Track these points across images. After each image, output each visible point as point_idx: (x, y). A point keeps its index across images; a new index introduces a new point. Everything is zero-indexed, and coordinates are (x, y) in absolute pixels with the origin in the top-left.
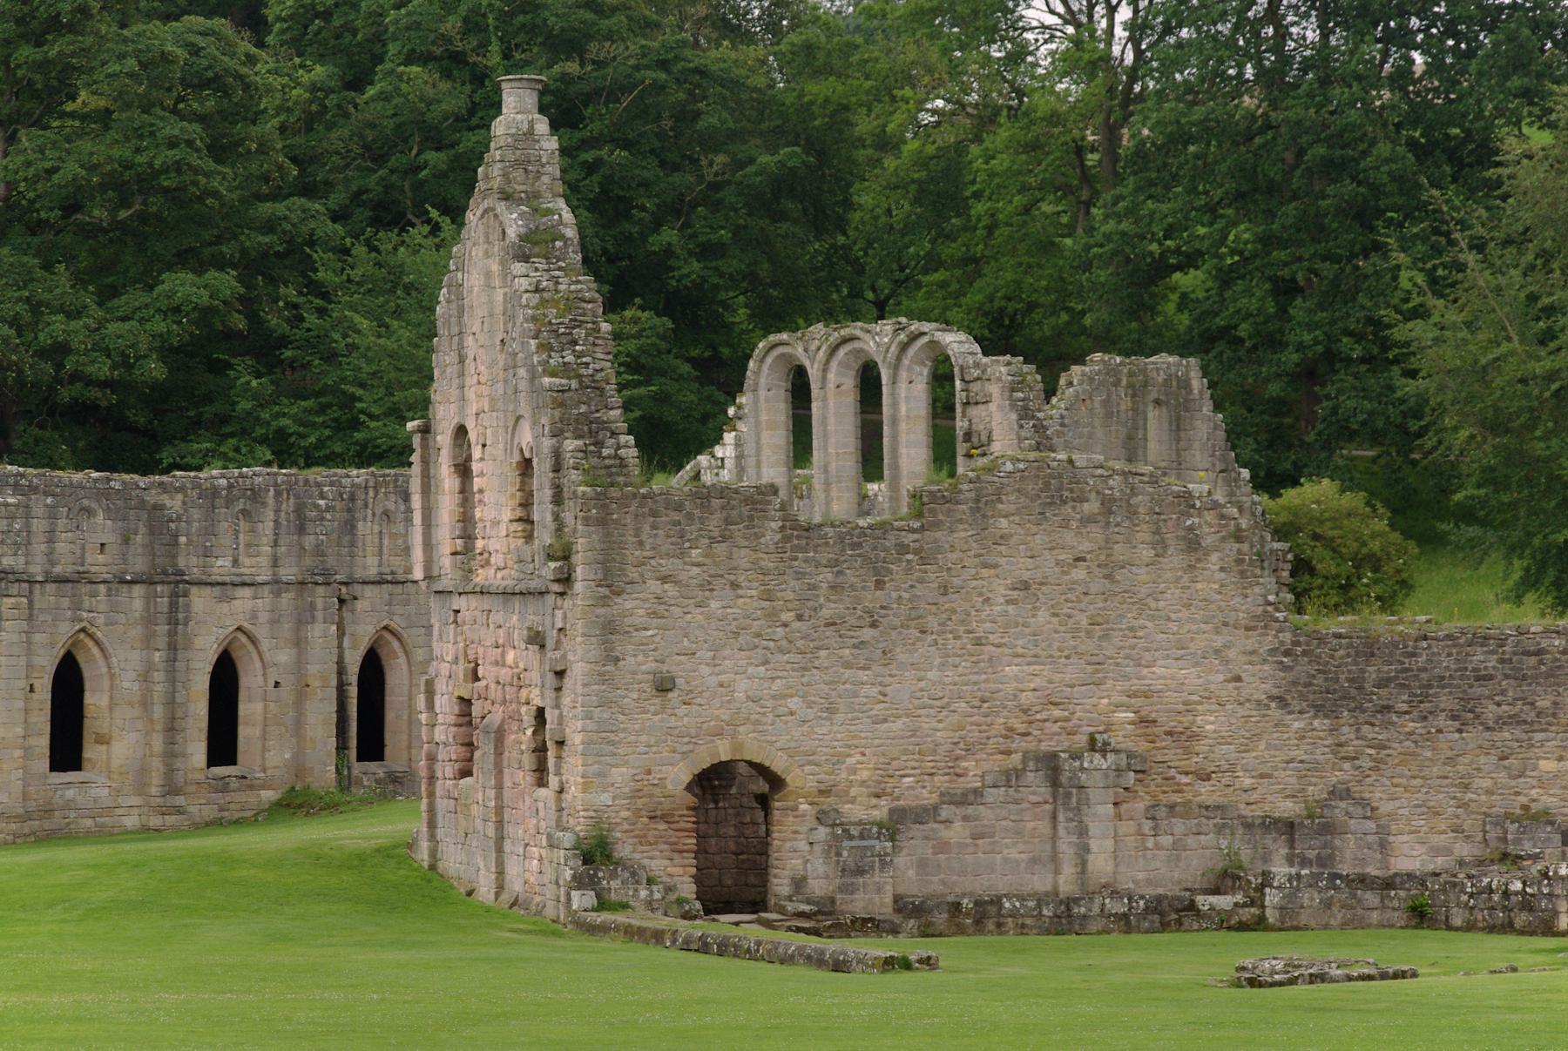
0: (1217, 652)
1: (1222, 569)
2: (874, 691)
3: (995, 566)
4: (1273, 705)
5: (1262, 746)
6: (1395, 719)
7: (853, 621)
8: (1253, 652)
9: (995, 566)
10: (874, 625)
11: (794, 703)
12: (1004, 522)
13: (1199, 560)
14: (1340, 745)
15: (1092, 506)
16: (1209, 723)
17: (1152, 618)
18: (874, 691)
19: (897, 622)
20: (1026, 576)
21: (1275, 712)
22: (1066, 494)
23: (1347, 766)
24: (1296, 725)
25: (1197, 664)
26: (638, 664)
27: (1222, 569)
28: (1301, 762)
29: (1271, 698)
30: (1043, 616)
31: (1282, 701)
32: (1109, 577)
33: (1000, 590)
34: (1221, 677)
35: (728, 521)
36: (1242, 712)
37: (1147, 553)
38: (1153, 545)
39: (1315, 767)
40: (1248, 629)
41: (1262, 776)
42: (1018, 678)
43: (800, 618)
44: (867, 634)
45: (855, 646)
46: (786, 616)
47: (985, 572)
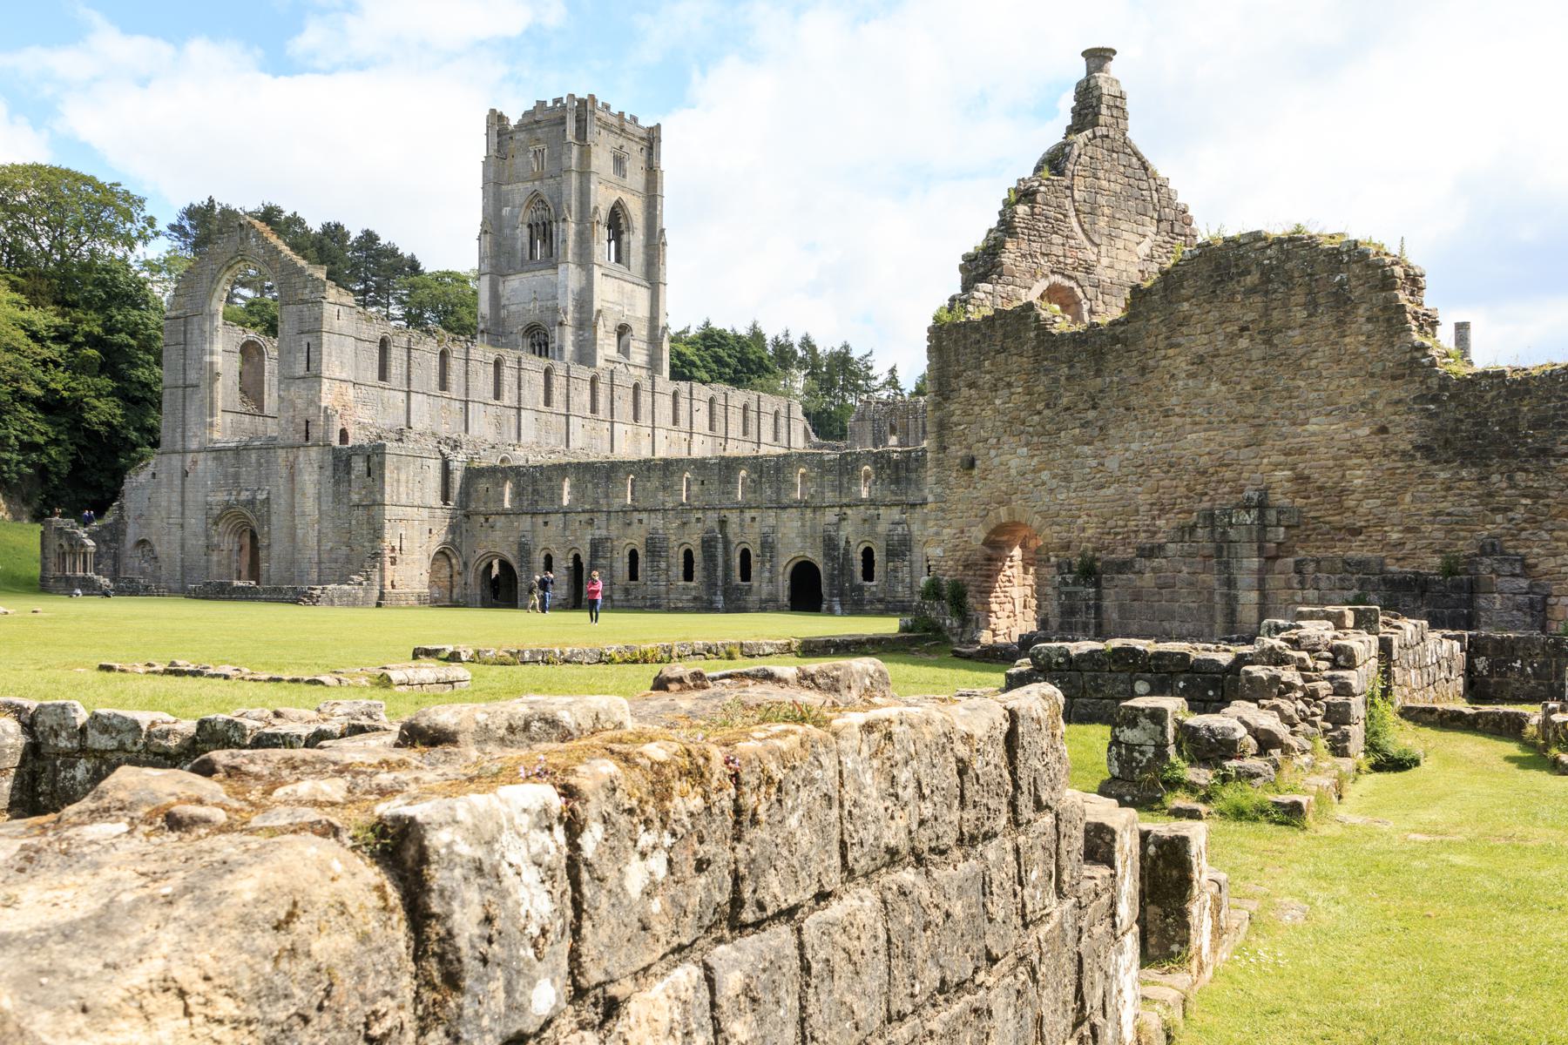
0: (1363, 404)
1: (1369, 320)
2: (1094, 463)
3: (1179, 345)
4: (1418, 455)
5: (1408, 498)
6: (1553, 463)
7: (1081, 406)
8: (1400, 401)
9: (1179, 345)
10: (1094, 408)
11: (1045, 475)
12: (1186, 306)
13: (1347, 313)
14: (1490, 495)
15: (1252, 279)
16: (1358, 478)
17: (1306, 378)
18: (1094, 463)
19: (1110, 403)
20: (1202, 350)
21: (1421, 464)
22: (1233, 270)
23: (1499, 518)
24: (1442, 475)
25: (1345, 418)
26: (957, 451)
27: (1369, 320)
28: (1449, 514)
29: (1417, 448)
30: (1215, 385)
31: (1427, 450)
32: (1268, 342)
33: (1182, 363)
34: (1366, 431)
35: (1005, 336)
36: (1387, 464)
37: (1300, 315)
38: (1305, 306)
39: (1464, 521)
40: (1394, 378)
41: (1408, 530)
42: (1195, 443)
43: (1047, 406)
44: (1091, 414)
45: (1082, 426)
46: (1040, 406)
47: (1171, 352)
